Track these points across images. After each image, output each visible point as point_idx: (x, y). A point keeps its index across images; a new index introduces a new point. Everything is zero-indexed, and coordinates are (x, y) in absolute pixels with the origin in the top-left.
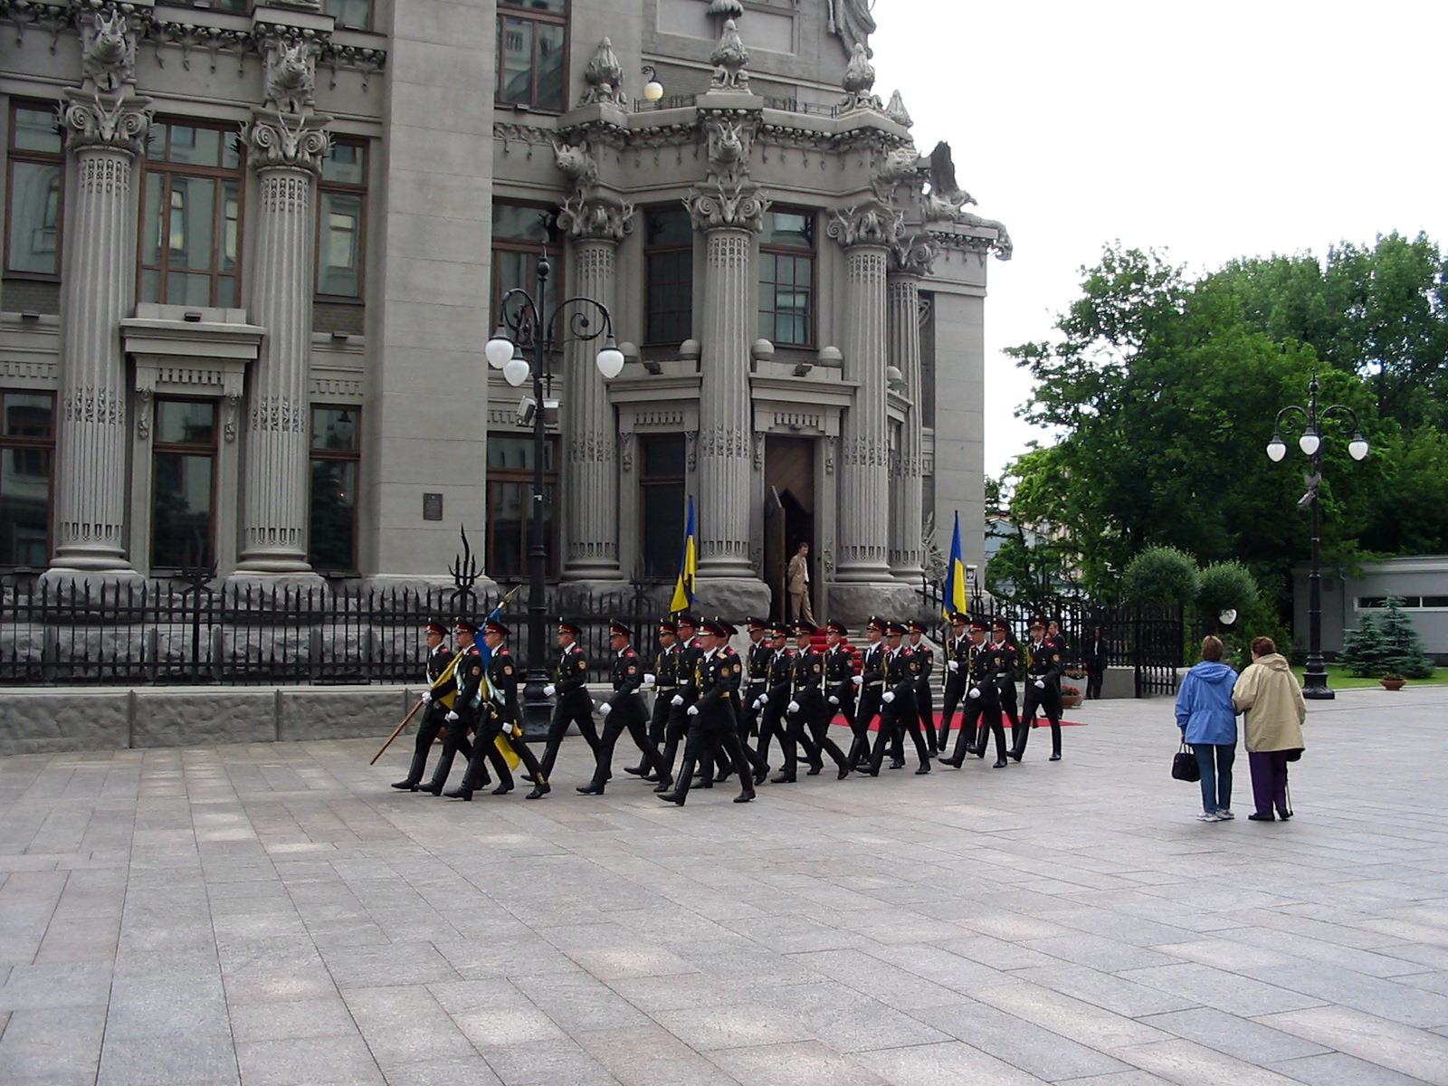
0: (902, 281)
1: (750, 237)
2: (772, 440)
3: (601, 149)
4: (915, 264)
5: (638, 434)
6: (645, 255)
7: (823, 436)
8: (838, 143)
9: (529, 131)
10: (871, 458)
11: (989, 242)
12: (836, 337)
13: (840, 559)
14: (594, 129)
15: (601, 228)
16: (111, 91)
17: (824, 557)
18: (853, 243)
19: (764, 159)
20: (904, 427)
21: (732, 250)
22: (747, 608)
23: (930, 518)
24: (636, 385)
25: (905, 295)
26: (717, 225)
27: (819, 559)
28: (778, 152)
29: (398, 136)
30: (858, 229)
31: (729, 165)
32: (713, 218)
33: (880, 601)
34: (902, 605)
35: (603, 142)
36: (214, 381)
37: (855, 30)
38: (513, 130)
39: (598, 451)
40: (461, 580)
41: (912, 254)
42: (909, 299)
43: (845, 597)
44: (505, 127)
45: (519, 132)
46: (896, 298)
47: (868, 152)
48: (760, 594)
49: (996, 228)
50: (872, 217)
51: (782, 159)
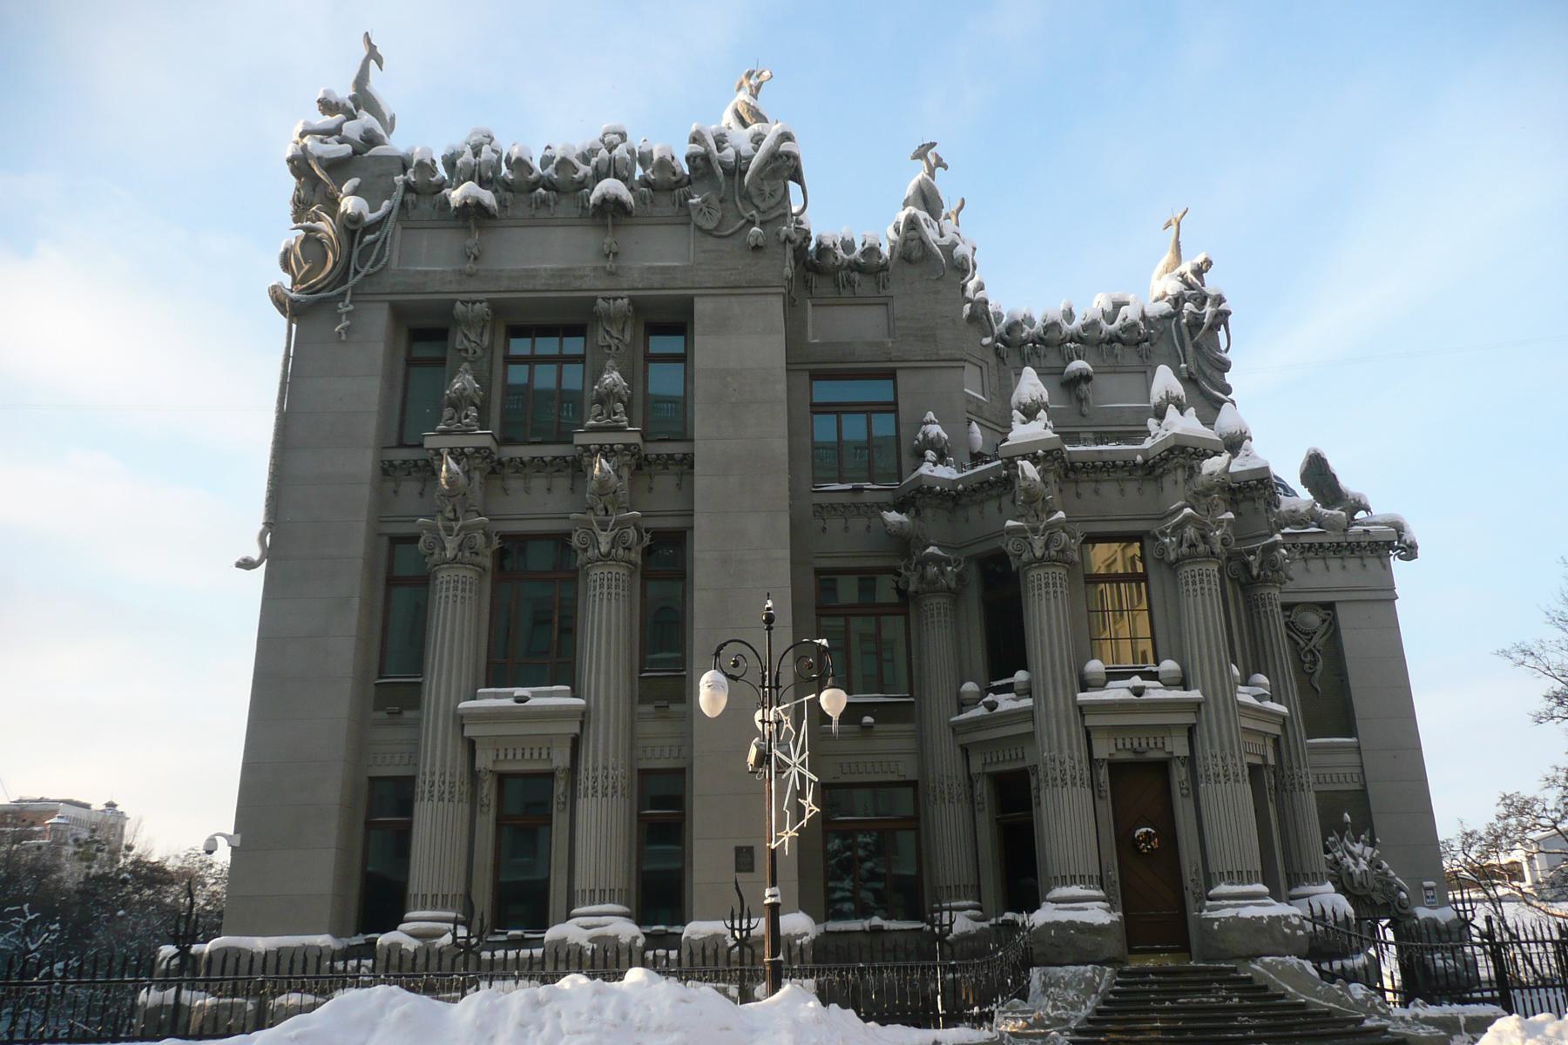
2: (1116, 767)
8: (1154, 466)
11: (1389, 545)
16: (456, 519)
18: (1178, 560)
19: (1078, 495)
20: (1282, 740)
21: (1047, 585)
25: (1264, 605)
26: (1030, 563)
28: (1093, 485)
29: (700, 522)
32: (1025, 557)
36: (544, 756)
37: (1208, 372)
40: (737, 934)
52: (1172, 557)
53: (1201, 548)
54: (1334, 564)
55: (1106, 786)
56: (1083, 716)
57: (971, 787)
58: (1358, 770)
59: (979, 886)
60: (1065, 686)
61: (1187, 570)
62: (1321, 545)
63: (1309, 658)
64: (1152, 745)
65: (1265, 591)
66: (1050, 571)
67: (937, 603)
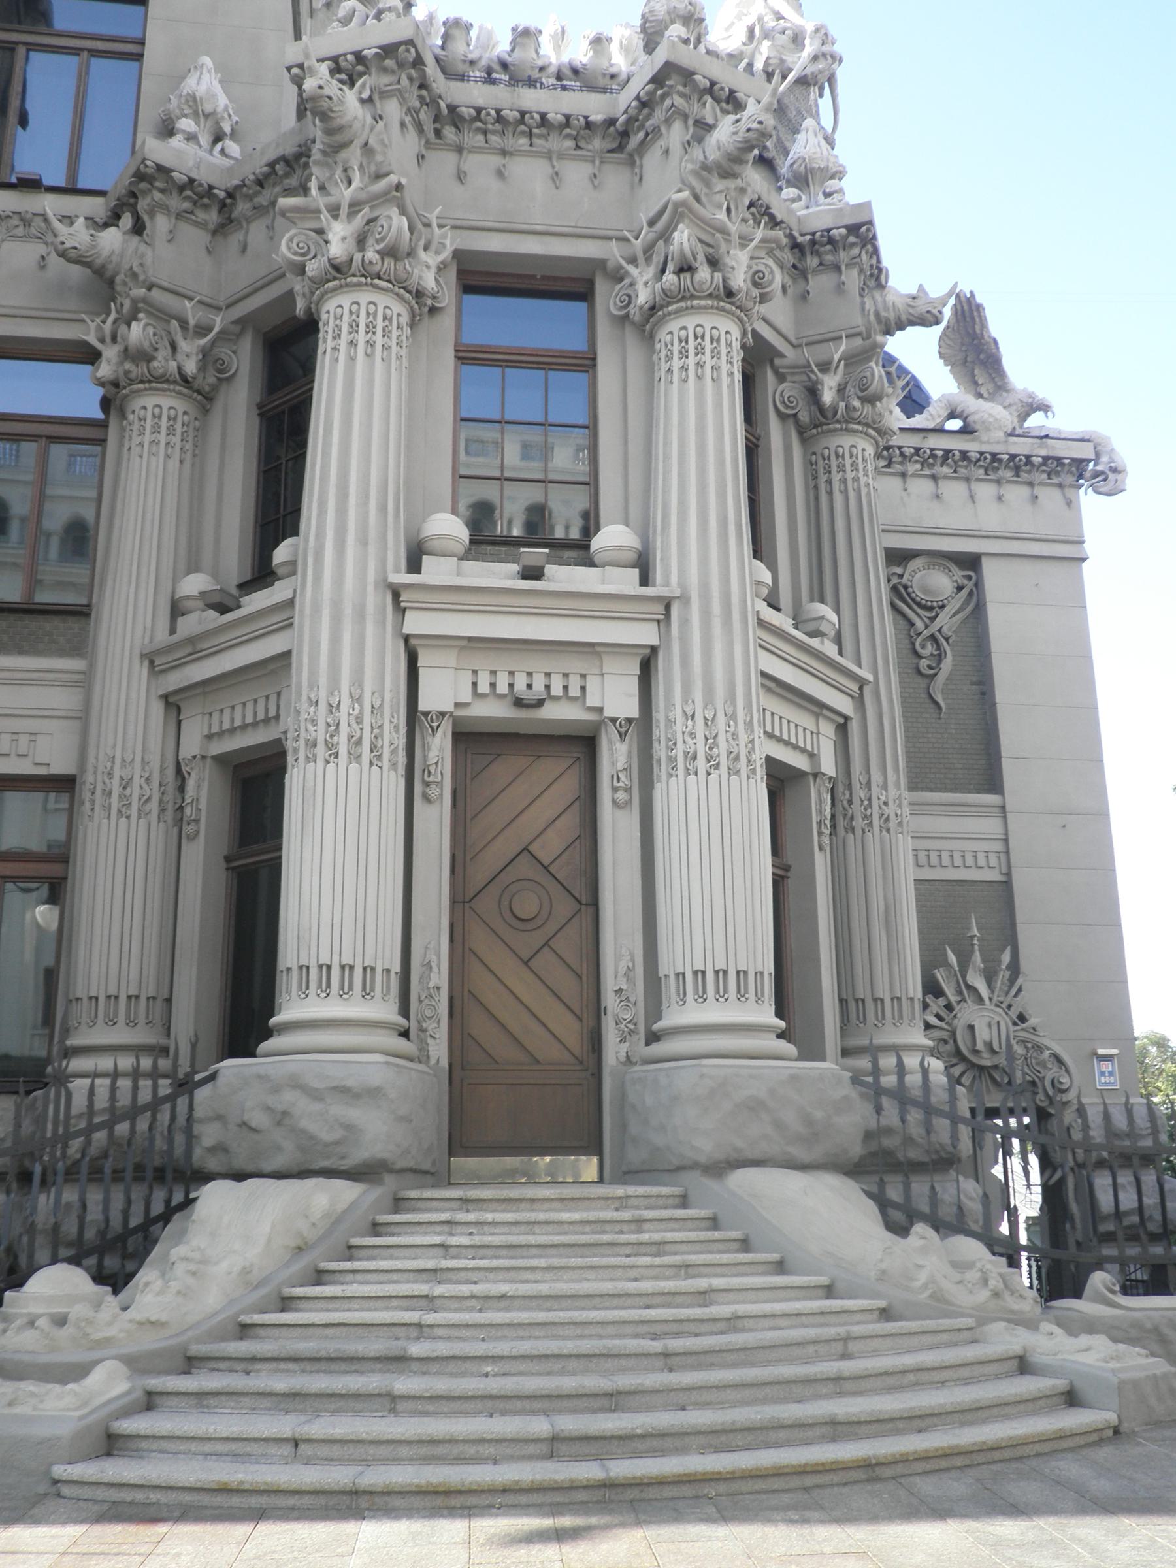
1: (413, 315)
5: (221, 760)
6: (261, 415)
13: (654, 1009)
14: (143, 185)
15: (142, 356)
19: (461, 176)
20: (854, 727)
22: (338, 1134)
23: (1006, 957)
25: (841, 469)
28: (496, 160)
31: (343, 155)
34: (808, 1121)
35: (166, 209)
38: (15, 221)
41: (851, 391)
42: (850, 475)
46: (823, 478)
47: (677, 126)
49: (1088, 441)
50: (683, 237)
53: (704, 273)
54: (985, 491)
56: (400, 611)
57: (181, 789)
58: (999, 846)
59: (169, 1001)
60: (363, 542)
61: (672, 329)
62: (964, 455)
63: (929, 649)
64: (557, 690)
65: (846, 441)
66: (364, 297)
67: (156, 407)
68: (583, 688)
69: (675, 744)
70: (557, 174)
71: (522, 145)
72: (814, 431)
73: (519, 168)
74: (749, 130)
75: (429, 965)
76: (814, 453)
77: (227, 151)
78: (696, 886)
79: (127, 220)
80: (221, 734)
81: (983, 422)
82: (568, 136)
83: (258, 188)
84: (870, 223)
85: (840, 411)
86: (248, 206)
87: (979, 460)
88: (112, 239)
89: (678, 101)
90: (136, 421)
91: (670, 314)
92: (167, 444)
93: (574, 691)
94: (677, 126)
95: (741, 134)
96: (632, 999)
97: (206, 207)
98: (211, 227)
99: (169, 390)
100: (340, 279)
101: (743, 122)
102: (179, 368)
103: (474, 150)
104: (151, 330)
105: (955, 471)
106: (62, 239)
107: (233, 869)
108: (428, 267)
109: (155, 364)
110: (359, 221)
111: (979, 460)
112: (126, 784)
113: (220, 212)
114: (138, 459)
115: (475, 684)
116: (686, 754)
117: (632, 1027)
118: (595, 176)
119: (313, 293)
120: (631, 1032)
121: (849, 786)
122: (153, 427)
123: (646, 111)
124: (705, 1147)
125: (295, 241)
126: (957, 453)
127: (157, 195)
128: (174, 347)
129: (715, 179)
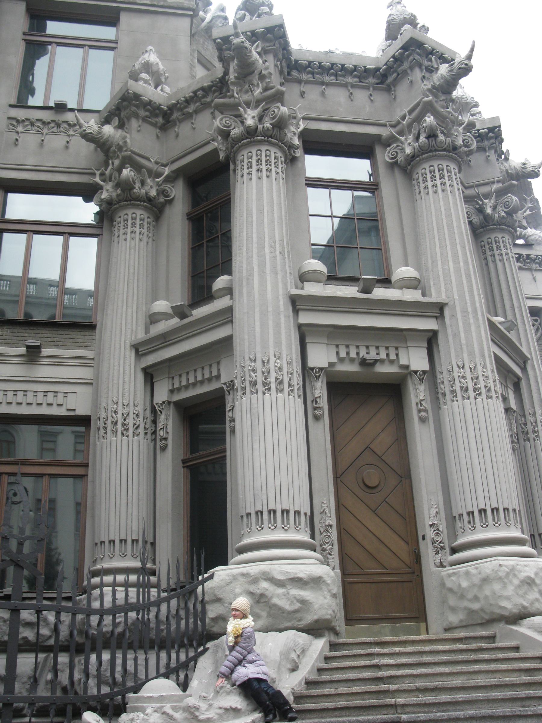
0: (493, 236)
3: (134, 123)
4: (503, 214)
5: (177, 404)
7: (408, 372)
8: (385, 76)
9: (69, 125)
10: (475, 390)
12: (410, 259)
13: (453, 535)
14: (125, 103)
17: (430, 534)
18: (413, 157)
19: (302, 94)
20: (523, 384)
21: (259, 162)
22: (297, 606)
24: (166, 339)
25: (499, 248)
27: (424, 538)
30: (417, 138)
31: (249, 78)
33: (516, 582)
35: (137, 116)
39: (123, 425)
41: (499, 208)
42: (504, 252)
43: (465, 584)
44: (44, 123)
45: (58, 125)
46: (489, 253)
47: (417, 71)
48: (315, 582)
50: (430, 119)
51: (323, 94)
52: (408, 151)
55: (324, 402)
57: (154, 422)
59: (153, 544)
60: (275, 273)
61: (425, 169)
62: (528, 256)
65: (500, 236)
68: (397, 355)
69: (454, 383)
70: (351, 94)
71: (333, 80)
72: (482, 230)
73: (331, 92)
74: (460, 68)
75: (323, 512)
76: (483, 241)
77: (164, 90)
78: (476, 461)
79: (116, 121)
80: (179, 389)
81: (537, 240)
82: (355, 76)
83: (186, 104)
84: (500, 126)
85: (496, 219)
86: (179, 113)
87: (536, 259)
88: (108, 129)
89: (417, 57)
90: (122, 221)
91: (423, 159)
92: (140, 233)
93: (393, 357)
94: (417, 71)
95: (455, 71)
96: (441, 529)
97: (156, 116)
98: (159, 125)
99: (141, 205)
100: (250, 139)
101: (456, 65)
102: (147, 193)
103: (307, 82)
104: (133, 174)
105: (524, 265)
106: (84, 128)
107: (187, 467)
108: (295, 134)
109: (135, 191)
110: (260, 109)
111: (536, 259)
112: (125, 417)
113: (163, 118)
114: (124, 242)
115: (338, 353)
116: (461, 388)
117: (442, 545)
118: (371, 95)
119: (233, 147)
120: (442, 548)
121: (524, 416)
122: (132, 224)
123: (398, 63)
124: (508, 606)
125: (224, 120)
126: (525, 255)
127: (134, 108)
128: (143, 183)
129: (440, 94)
